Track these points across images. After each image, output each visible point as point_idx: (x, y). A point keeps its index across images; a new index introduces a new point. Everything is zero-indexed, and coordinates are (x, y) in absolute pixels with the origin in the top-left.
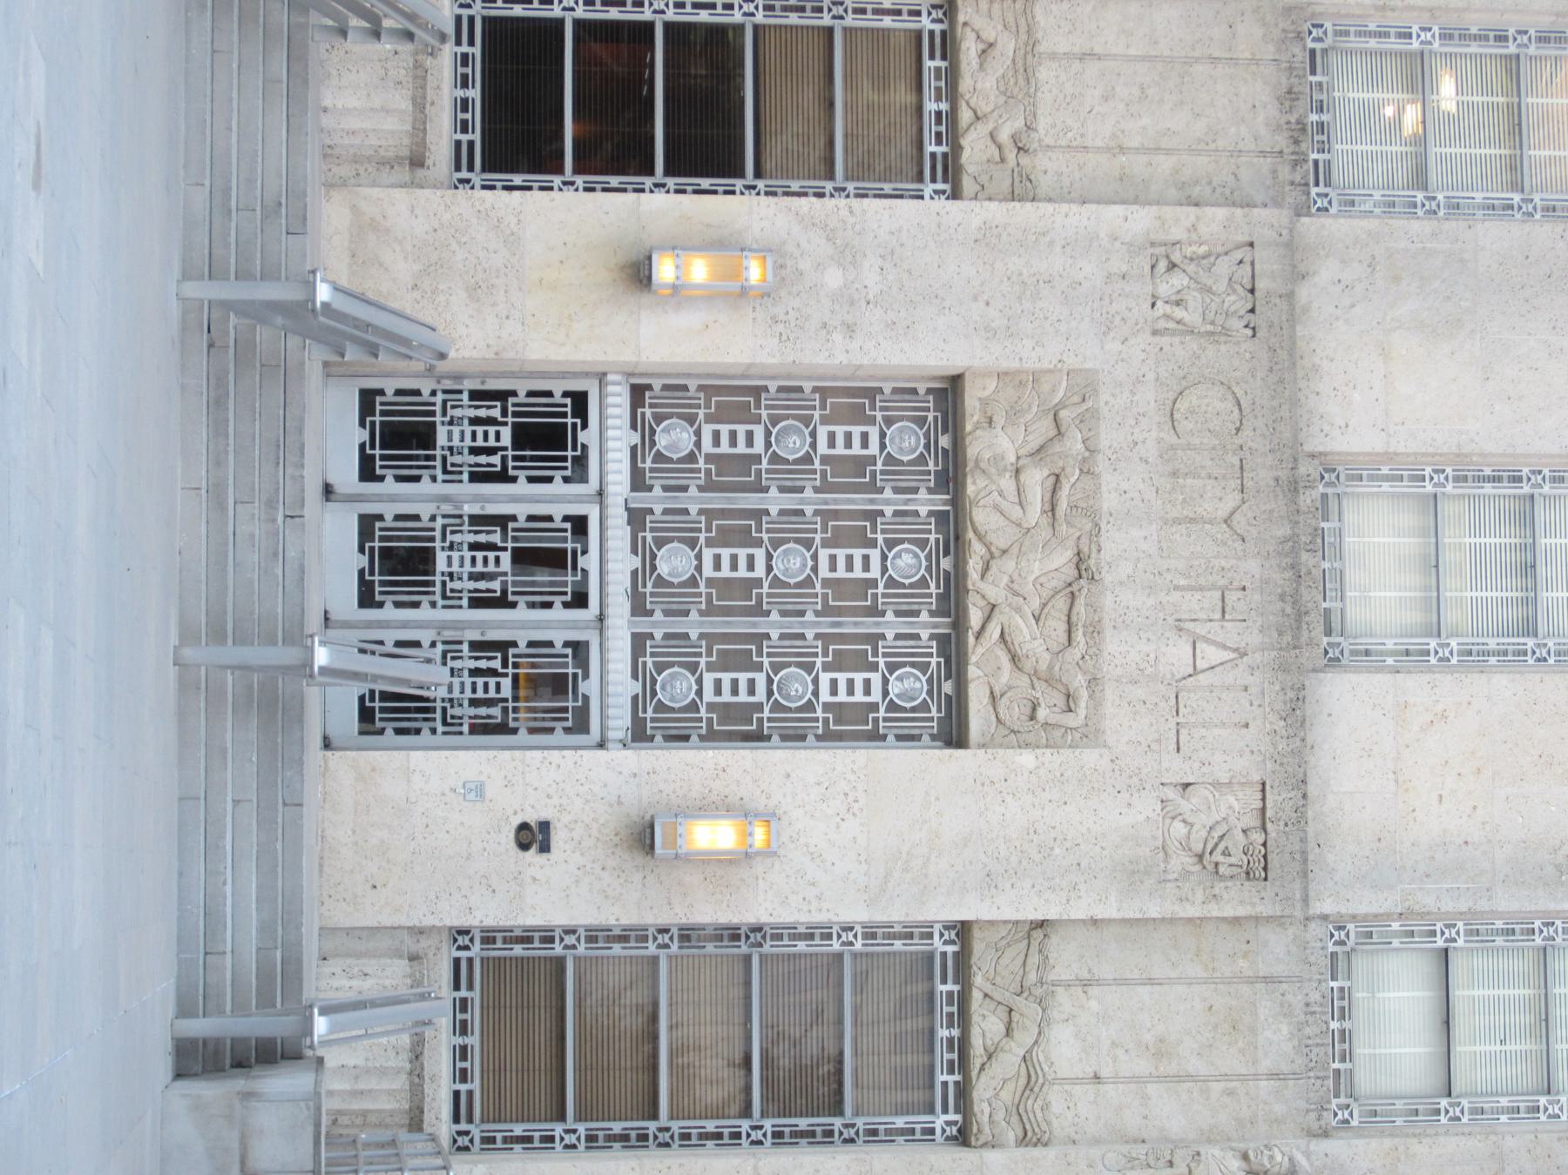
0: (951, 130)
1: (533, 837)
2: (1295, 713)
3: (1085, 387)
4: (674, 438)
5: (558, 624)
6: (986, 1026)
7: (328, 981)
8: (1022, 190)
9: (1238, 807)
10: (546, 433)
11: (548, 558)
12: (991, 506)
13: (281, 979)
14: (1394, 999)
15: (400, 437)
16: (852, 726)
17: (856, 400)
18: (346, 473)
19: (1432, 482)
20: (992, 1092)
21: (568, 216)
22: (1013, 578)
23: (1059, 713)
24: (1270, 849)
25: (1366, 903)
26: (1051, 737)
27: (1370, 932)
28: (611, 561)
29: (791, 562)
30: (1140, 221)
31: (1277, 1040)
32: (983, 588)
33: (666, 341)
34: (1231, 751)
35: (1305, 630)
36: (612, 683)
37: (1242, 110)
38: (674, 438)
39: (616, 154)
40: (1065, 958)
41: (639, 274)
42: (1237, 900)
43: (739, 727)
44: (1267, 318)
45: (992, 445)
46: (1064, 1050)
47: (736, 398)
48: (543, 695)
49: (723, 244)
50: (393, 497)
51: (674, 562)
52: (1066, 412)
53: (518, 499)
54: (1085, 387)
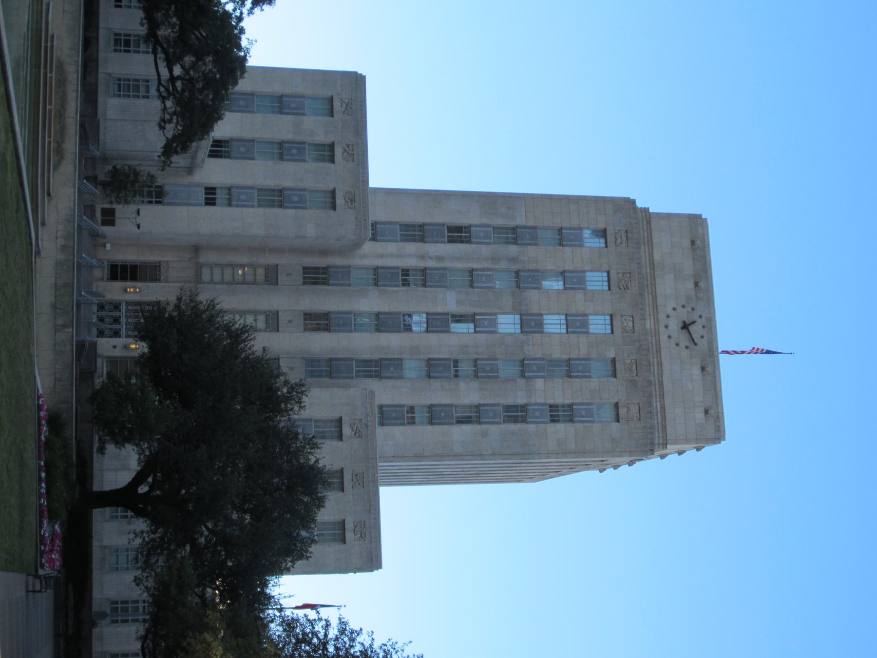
0: (160, 275)
1: (115, 347)
4: (130, 308)
8: (167, 281)
10: (117, 306)
11: (117, 320)
15: (101, 307)
18: (95, 311)
21: (118, 285)
28: (123, 320)
30: (179, 285)
33: (128, 297)
36: (123, 332)
38: (130, 308)
39: (124, 279)
41: (126, 291)
48: (116, 334)
49: (135, 288)
50: (101, 314)
51: (130, 320)
53: (114, 314)
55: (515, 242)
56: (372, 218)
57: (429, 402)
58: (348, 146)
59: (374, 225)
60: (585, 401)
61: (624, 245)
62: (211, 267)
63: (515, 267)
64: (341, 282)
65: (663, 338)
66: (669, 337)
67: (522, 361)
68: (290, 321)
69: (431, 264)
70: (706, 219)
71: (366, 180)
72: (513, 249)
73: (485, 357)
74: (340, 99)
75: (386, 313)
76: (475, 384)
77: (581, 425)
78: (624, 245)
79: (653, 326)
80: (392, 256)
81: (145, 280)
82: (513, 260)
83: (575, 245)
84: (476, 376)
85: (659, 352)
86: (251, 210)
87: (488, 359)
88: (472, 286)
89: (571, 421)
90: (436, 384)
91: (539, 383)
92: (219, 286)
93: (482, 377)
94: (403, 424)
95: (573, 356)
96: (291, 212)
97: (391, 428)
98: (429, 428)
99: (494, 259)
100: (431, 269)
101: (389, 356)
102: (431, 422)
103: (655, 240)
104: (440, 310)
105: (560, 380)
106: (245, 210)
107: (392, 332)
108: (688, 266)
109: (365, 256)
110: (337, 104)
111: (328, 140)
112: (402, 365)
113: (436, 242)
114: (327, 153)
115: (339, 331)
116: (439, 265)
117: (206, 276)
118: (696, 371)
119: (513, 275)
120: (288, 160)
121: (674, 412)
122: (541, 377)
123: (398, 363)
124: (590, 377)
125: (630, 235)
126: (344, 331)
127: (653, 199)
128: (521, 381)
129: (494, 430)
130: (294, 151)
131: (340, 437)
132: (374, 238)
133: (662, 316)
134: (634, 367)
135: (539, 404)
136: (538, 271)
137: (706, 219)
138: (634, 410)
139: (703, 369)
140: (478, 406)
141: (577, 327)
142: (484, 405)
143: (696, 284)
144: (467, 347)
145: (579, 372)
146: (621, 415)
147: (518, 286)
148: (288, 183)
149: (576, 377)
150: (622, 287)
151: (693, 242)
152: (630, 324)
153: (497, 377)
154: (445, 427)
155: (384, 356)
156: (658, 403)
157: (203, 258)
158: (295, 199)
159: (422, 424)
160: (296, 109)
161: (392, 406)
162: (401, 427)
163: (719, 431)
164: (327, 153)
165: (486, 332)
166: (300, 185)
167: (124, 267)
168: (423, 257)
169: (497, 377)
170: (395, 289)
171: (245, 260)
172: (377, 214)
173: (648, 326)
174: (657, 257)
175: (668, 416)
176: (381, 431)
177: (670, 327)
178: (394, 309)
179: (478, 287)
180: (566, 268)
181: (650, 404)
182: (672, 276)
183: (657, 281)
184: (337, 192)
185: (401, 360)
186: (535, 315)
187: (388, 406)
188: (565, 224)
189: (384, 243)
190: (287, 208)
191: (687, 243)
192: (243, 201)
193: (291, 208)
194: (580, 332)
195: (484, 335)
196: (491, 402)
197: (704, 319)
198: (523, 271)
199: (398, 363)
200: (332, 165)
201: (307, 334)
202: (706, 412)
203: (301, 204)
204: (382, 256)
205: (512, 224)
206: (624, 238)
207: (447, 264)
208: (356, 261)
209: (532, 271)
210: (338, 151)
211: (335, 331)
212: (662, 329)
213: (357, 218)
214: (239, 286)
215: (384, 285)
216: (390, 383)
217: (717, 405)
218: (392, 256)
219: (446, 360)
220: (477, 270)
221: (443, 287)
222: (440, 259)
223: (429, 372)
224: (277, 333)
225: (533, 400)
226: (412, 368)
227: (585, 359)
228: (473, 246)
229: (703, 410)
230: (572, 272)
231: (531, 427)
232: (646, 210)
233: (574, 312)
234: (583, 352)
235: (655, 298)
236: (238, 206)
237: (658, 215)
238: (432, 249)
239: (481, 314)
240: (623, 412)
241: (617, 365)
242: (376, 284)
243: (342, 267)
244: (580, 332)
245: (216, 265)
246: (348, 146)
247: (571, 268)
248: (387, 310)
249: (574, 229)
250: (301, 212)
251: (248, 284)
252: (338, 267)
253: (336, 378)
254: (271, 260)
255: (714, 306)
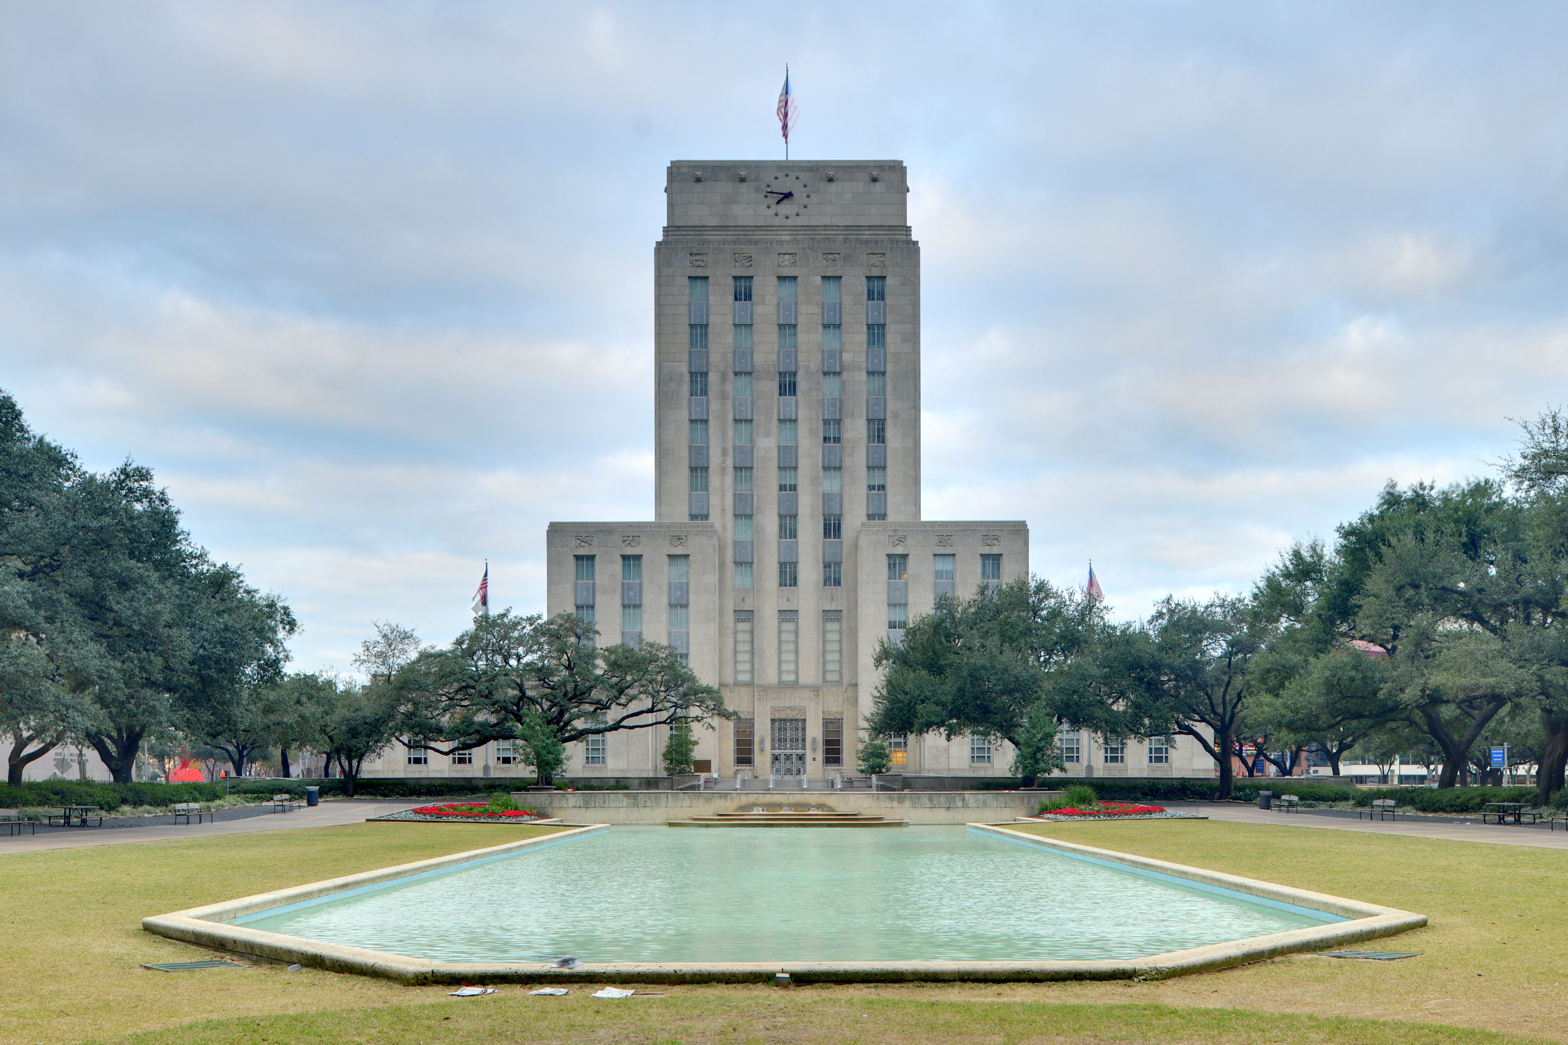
1: (814, 759)
2: (804, 687)
3: (772, 707)
4: (777, 746)
5: (794, 757)
6: (832, 717)
7: (827, 778)
9: (812, 693)
10: (776, 758)
11: (788, 757)
12: (783, 716)
13: (827, 781)
14: (831, 677)
16: (804, 729)
17: (773, 729)
19: (780, 672)
20: (838, 717)
21: (757, 757)
22: (791, 715)
23: (803, 710)
24: (815, 689)
25: (821, 680)
26: (805, 711)
27: (824, 679)
28: (788, 752)
29: (788, 735)
30: (756, 702)
31: (834, 689)
32: (791, 717)
34: (806, 694)
35: (795, 685)
36: (800, 752)
37: (744, 691)
38: (777, 746)
39: (750, 751)
40: (826, 709)
42: (821, 694)
43: (804, 740)
44: (765, 689)
45: (777, 716)
46: (835, 710)
47: (773, 740)
48: (801, 758)
51: (788, 746)
52: (774, 709)
53: (782, 760)
54: (772, 707)
55: (705, 374)
56: (686, 519)
57: (865, 469)
58: (624, 541)
59: (693, 517)
60: (865, 310)
61: (705, 258)
62: (736, 672)
63: (731, 375)
64: (749, 550)
65: (799, 221)
66: (798, 215)
67: (825, 374)
68: (788, 599)
69: (730, 463)
70: (672, 162)
71: (651, 523)
72: (713, 377)
73: (821, 411)
74: (575, 547)
75: (779, 508)
76: (847, 423)
77: (888, 317)
78: (705, 258)
79: (788, 233)
80: (723, 500)
81: (752, 734)
82: (724, 378)
83: (707, 311)
84: (838, 422)
85: (814, 228)
86: (691, 635)
87: (823, 409)
88: (751, 421)
89: (883, 326)
90: (847, 461)
91: (847, 357)
92: (756, 665)
93: (840, 415)
94: (886, 494)
95: (820, 321)
96: (692, 598)
97: (889, 507)
98: (889, 469)
99: (723, 396)
100: (734, 461)
101: (821, 506)
102: (884, 468)
103: (696, 222)
104: (775, 455)
105: (844, 335)
106: (691, 641)
107: (797, 503)
108: (724, 187)
109: (724, 526)
110: (582, 552)
111: (619, 561)
112: (828, 494)
113: (708, 455)
114: (631, 561)
115: (797, 553)
116: (731, 454)
117: (791, 678)
118: (833, 187)
119: (738, 377)
120: (641, 599)
121: (874, 215)
122: (841, 356)
123: (827, 498)
124: (840, 304)
125: (695, 251)
126: (797, 549)
127: (654, 219)
128: (845, 375)
129: (892, 406)
130: (632, 594)
131: (905, 557)
132: (706, 517)
133: (777, 222)
134: (831, 256)
135: (867, 359)
136: (734, 351)
137: (672, 162)
138: (875, 259)
139: (831, 180)
140: (869, 420)
141: (791, 314)
142: (867, 414)
143: (743, 180)
144: (811, 429)
145: (835, 314)
146: (879, 274)
147: (750, 373)
148: (665, 600)
149: (840, 319)
150: (749, 264)
151: (698, 180)
152: (787, 257)
153: (841, 400)
154: (889, 454)
155: (821, 511)
156: (866, 232)
157: (730, 680)
158: (679, 593)
159: (885, 476)
160: (588, 591)
161: (868, 504)
162: (888, 497)
163: (894, 167)
164: (631, 561)
165: (797, 409)
166: (665, 588)
167: (738, 751)
168: (724, 469)
169: (841, 400)
170: (755, 498)
171: (730, 641)
172: (680, 513)
173: (787, 238)
174: (714, 222)
175: (878, 223)
176: (891, 517)
177: (788, 213)
178: (776, 498)
179: (752, 415)
180: (731, 322)
181: (867, 242)
182: (734, 206)
183: (739, 223)
184: (671, 553)
185: (824, 494)
186: (778, 358)
187: (868, 509)
188: (686, 320)
189: (711, 507)
190: (688, 601)
191: (699, 187)
192: (682, 643)
193: (688, 597)
194: (796, 312)
195: (800, 412)
196: (865, 408)
197: (779, 174)
198: (735, 368)
199: (827, 498)
200: (644, 556)
201: (800, 582)
202: (875, 180)
203: (685, 588)
204: (723, 510)
205: (687, 377)
206: (698, 257)
207: (730, 445)
208: (729, 537)
209: (734, 358)
210: (629, 551)
211: (797, 557)
212: (789, 222)
213: (696, 534)
214: (755, 646)
215: (752, 509)
216: (846, 506)
217: (868, 167)
218: (723, 500)
219: (823, 450)
220: (734, 415)
221: (752, 450)
222: (724, 453)
223: (835, 468)
224: (800, 612)
225: (863, 365)
226: (831, 484)
227: (823, 308)
228: (711, 418)
229: (872, 184)
230: (734, 316)
231: (889, 368)
232: (666, 230)
233: (775, 317)
234: (815, 309)
235: (758, 227)
236: (688, 648)
237: (671, 215)
238: (715, 460)
239: (779, 412)
240: (876, 272)
241: (829, 274)
242: (750, 516)
243: (735, 548)
244: (796, 312)
245: (735, 668)
246: (624, 541)
247: (731, 316)
248: (776, 507)
249: (690, 311)
250: (692, 588)
251: (753, 638)
252: (735, 553)
253: (841, 558)
254: (730, 616)
255: (765, 161)
